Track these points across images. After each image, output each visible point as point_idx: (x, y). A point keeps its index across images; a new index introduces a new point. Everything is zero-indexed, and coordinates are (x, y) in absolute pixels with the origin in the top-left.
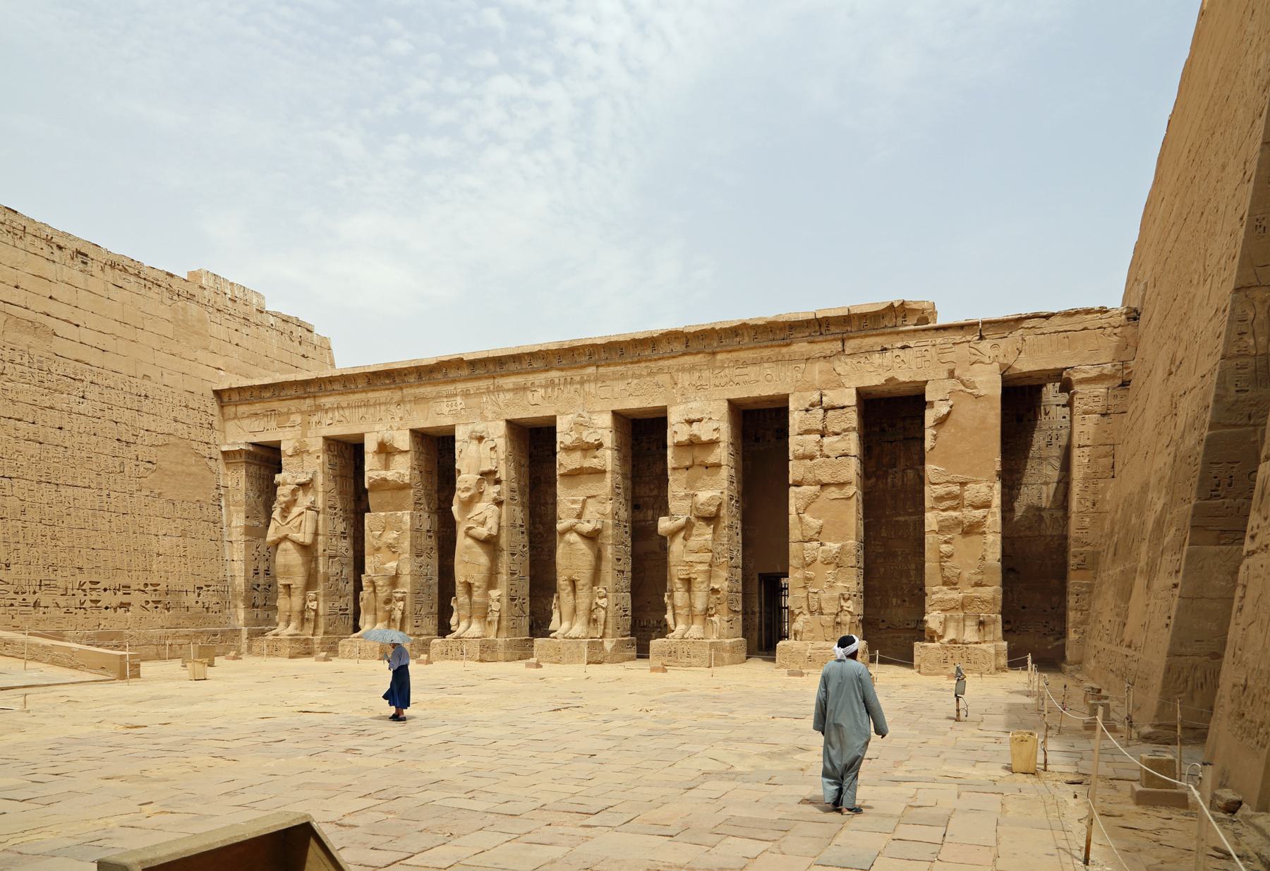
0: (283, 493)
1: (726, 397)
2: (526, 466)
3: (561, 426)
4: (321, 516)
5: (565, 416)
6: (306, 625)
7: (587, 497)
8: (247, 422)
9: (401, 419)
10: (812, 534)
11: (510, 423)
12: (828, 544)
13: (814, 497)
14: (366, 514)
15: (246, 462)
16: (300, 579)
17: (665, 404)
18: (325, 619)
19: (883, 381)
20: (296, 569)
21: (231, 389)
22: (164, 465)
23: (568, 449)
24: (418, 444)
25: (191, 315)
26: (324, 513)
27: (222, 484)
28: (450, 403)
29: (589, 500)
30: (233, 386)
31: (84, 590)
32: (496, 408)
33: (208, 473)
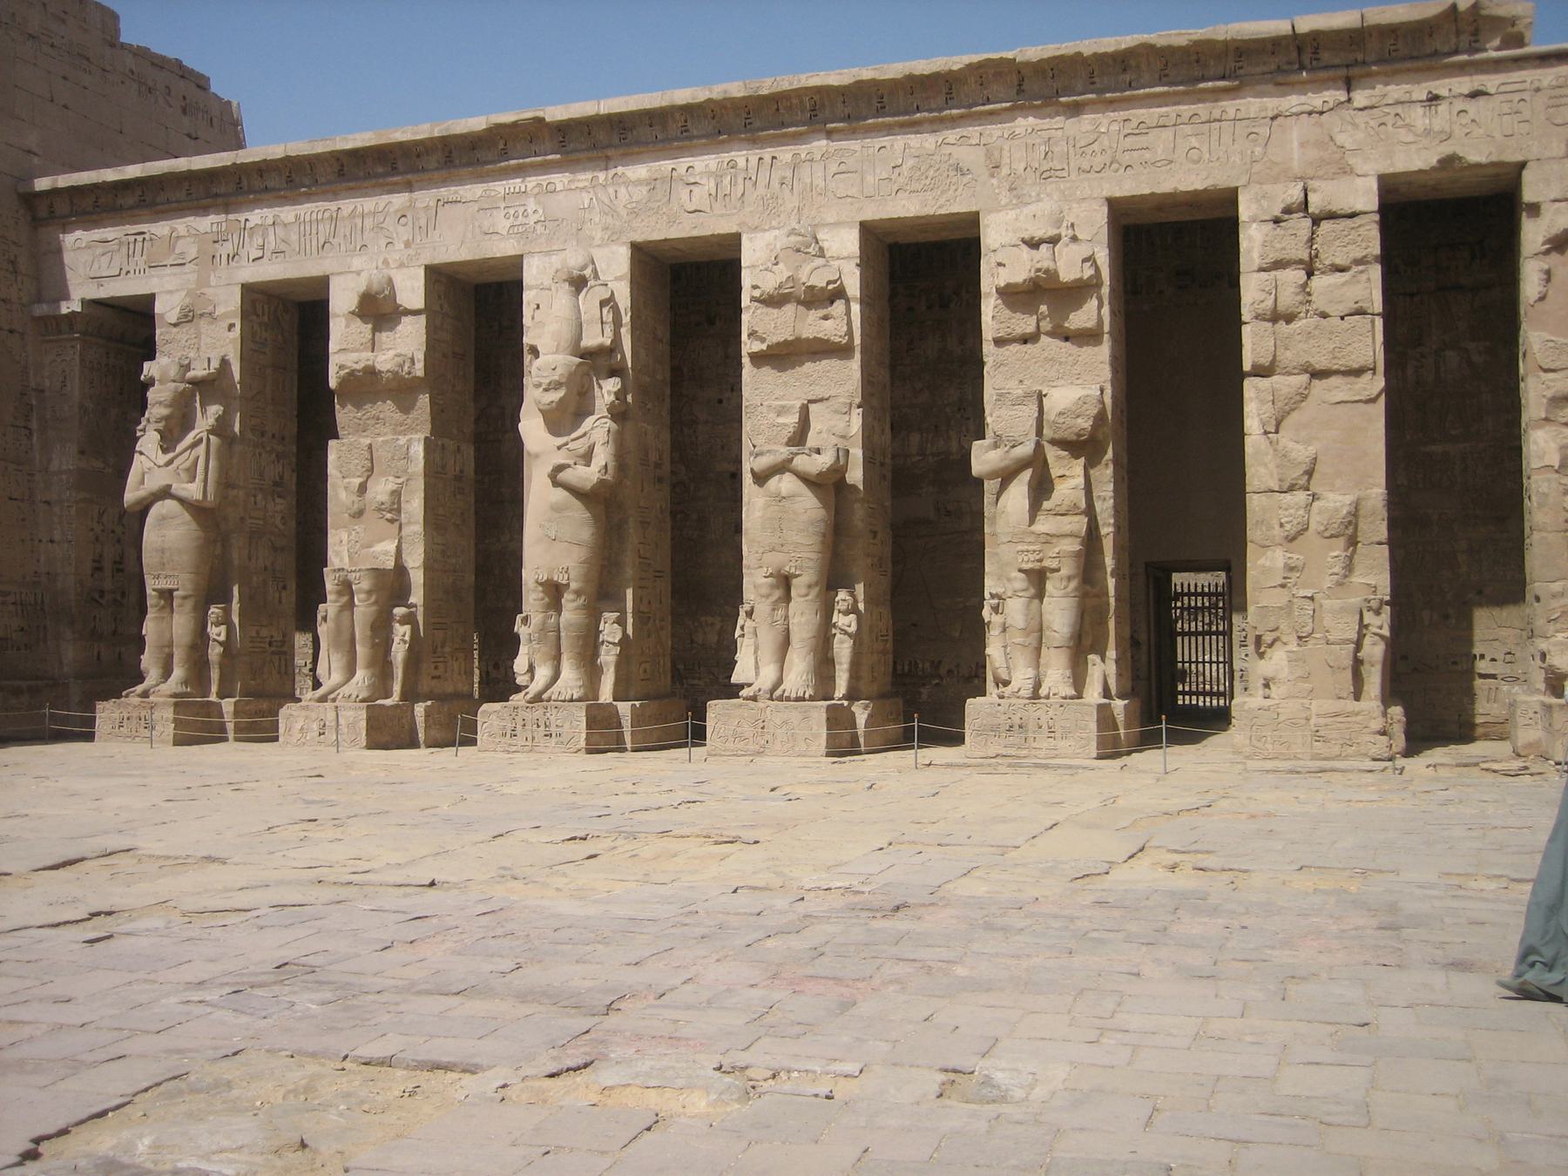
1: (1106, 193)
2: (665, 341)
3: (751, 253)
5: (759, 235)
7: (810, 401)
9: (407, 245)
10: (1294, 476)
11: (637, 248)
12: (1331, 496)
13: (1298, 398)
14: (332, 443)
17: (974, 209)
19: (1433, 161)
23: (774, 301)
24: (439, 297)
28: (512, 211)
29: (812, 407)
32: (609, 219)
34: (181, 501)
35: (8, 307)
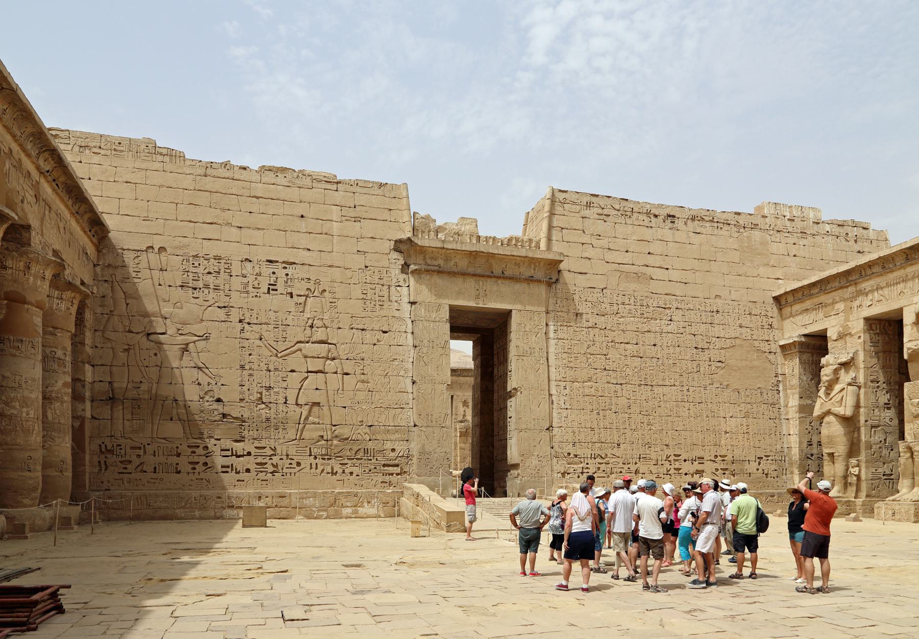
0: (826, 374)
4: (862, 390)
6: (849, 489)
8: (800, 317)
15: (800, 352)
16: (842, 447)
18: (867, 484)
20: (838, 439)
21: (786, 293)
22: (730, 362)
25: (755, 241)
26: (865, 387)
27: (780, 372)
30: (788, 290)
31: (669, 461)
33: (768, 365)
34: (836, 415)
35: (769, 343)
